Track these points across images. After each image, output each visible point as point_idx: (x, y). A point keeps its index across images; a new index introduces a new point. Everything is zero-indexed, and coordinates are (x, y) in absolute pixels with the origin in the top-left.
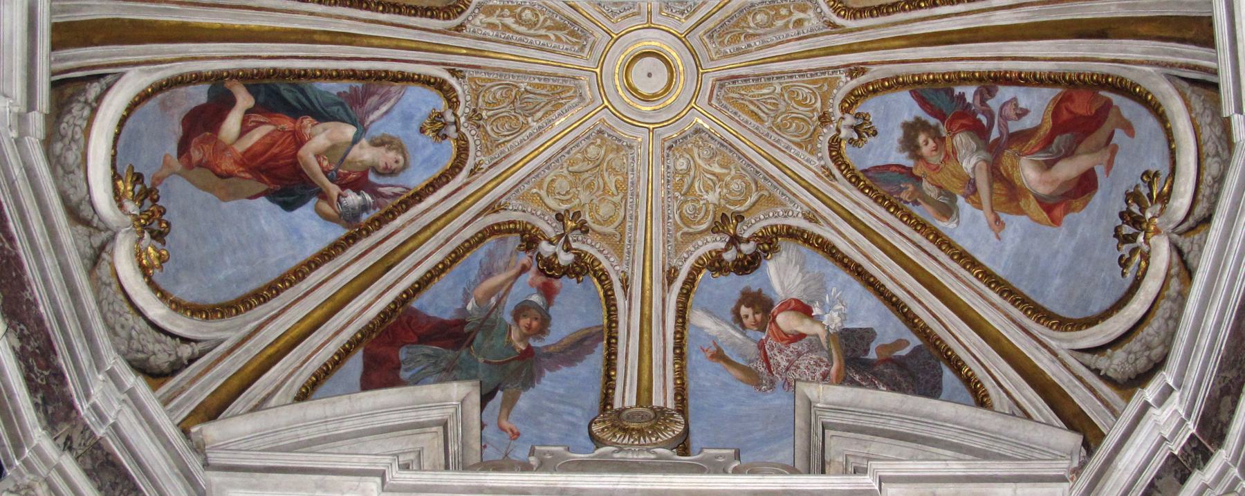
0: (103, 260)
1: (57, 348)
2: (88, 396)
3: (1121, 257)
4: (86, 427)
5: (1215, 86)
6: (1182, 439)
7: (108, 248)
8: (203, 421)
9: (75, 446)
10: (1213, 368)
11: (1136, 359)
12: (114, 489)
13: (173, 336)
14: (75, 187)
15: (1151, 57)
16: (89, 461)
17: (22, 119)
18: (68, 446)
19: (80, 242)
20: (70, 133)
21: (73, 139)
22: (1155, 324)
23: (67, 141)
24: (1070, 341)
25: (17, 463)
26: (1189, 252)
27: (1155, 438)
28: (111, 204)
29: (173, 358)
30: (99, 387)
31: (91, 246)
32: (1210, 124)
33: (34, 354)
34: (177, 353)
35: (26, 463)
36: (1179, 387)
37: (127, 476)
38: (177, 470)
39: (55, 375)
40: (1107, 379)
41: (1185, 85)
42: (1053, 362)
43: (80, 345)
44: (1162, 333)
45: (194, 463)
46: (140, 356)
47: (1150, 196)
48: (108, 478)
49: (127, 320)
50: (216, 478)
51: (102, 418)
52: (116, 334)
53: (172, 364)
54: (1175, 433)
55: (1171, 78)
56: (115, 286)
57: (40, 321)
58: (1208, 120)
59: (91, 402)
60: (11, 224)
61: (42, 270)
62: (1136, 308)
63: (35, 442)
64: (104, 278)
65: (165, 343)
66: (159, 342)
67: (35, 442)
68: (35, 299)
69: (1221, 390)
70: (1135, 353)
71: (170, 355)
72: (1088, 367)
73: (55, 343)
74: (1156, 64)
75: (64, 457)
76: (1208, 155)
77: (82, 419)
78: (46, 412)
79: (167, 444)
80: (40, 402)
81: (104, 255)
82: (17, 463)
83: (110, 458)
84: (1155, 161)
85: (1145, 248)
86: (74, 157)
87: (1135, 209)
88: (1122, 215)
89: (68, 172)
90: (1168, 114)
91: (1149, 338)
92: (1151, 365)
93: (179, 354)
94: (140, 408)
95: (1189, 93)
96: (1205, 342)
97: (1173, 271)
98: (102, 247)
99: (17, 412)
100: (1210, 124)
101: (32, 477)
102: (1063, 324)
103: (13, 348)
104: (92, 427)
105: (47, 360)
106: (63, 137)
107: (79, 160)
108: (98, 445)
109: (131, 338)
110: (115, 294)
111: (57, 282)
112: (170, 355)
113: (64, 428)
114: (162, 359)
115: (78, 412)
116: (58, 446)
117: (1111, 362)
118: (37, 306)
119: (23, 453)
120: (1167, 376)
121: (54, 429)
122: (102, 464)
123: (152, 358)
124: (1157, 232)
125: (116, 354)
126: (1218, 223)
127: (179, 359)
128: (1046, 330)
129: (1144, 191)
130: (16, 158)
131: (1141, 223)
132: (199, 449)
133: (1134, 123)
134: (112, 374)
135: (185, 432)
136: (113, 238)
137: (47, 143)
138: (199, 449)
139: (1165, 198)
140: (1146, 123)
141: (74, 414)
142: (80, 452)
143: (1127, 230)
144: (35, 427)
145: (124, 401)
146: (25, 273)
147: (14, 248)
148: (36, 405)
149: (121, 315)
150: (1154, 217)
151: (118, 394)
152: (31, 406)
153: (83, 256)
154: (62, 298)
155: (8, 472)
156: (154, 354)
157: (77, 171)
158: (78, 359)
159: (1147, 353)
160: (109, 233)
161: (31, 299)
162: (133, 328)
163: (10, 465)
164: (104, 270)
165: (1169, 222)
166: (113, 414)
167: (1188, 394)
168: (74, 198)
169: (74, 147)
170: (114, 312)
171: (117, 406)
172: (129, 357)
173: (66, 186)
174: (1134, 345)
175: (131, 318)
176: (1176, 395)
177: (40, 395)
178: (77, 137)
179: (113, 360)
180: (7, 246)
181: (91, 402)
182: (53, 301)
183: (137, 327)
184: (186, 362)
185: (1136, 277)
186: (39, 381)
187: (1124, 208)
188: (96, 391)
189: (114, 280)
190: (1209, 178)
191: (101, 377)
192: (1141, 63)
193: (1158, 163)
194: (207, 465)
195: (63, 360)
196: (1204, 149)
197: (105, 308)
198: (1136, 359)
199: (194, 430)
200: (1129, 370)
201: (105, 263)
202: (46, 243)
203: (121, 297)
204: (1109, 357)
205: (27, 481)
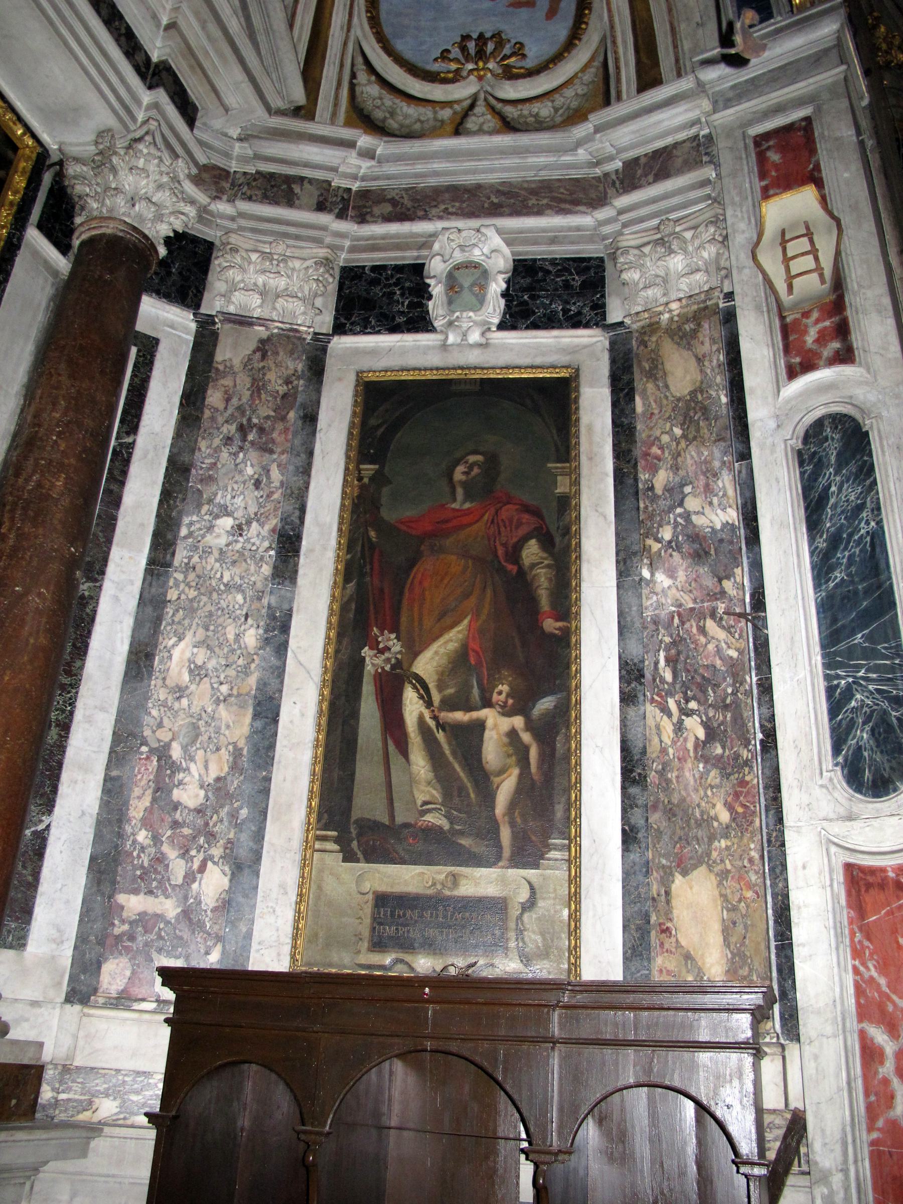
3: (447, 51)
5: (607, 103)
6: (345, 184)
10: (405, 183)
11: (378, 107)
15: (616, 19)
22: (410, 111)
24: (365, 36)
26: (474, 115)
27: (335, 162)
32: (577, 94)
36: (379, 162)
40: (352, 88)
41: (601, 58)
42: (342, 28)
44: (407, 122)
47: (505, 57)
54: (345, 176)
55: (603, 40)
58: (580, 92)
62: (416, 87)
69: (393, 199)
70: (383, 104)
72: (353, 65)
74: (612, 27)
76: (553, 101)
84: (534, 49)
85: (464, 74)
87: (490, 47)
88: (481, 36)
90: (574, 52)
91: (398, 111)
92: (380, 124)
95: (596, 64)
96: (420, 168)
97: (456, 106)
100: (577, 94)
102: (374, 21)
117: (366, 85)
120: (382, 147)
124: (480, 78)
126: (506, 140)
128: (363, 9)
129: (507, 50)
131: (481, 58)
133: (558, 16)
139: (509, 74)
140: (561, 29)
143: (471, 46)
150: (490, 70)
159: (388, 115)
165: (492, 87)
167: (377, 171)
174: (389, 100)
176: (373, 163)
185: (438, 73)
187: (488, 35)
190: (536, 110)
192: (609, 10)
193: (535, 53)
196: (557, 96)
198: (378, 107)
200: (369, 105)
204: (369, 81)
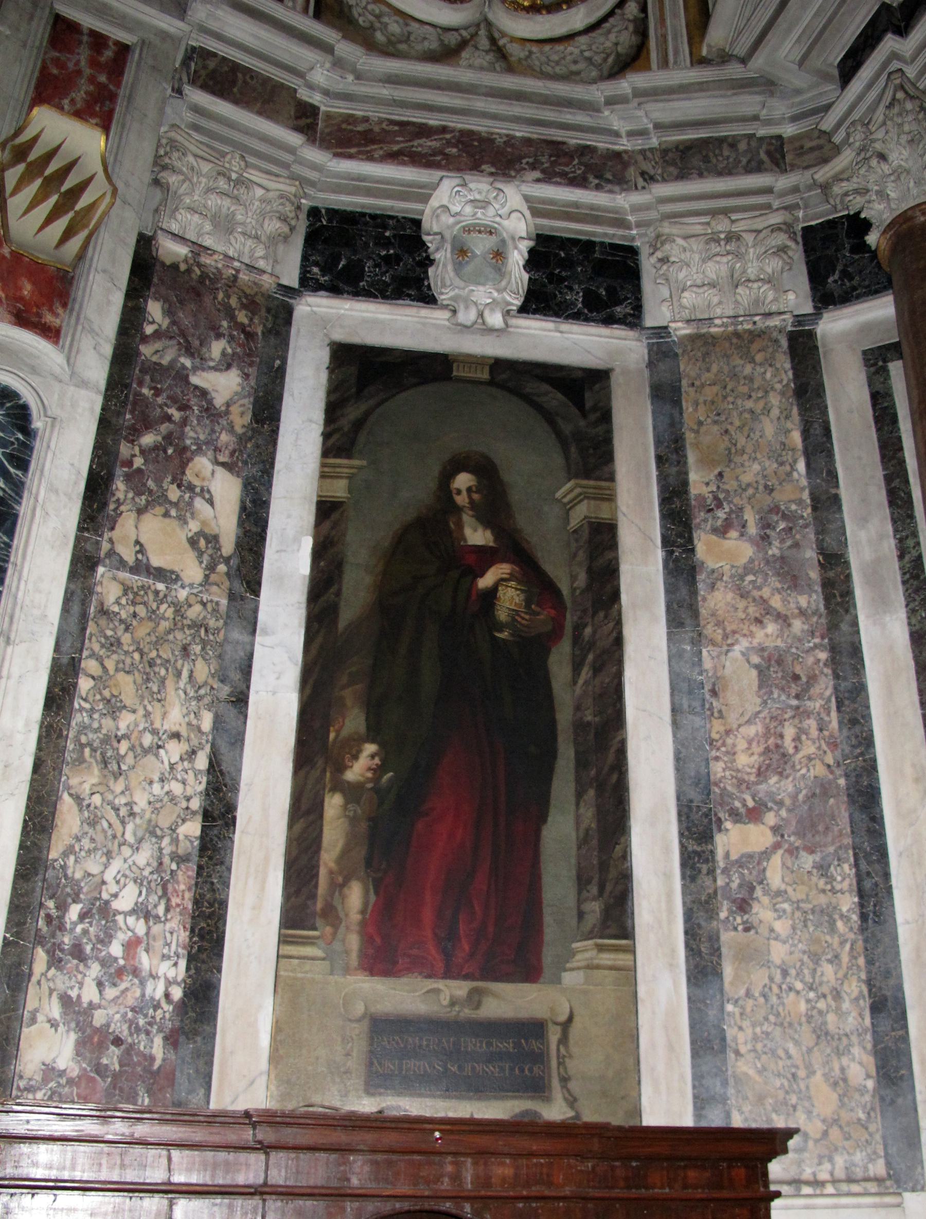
0: (504, 46)
1: (560, 139)
2: (617, 134)
4: (643, 152)
7: (496, 35)
8: (702, 41)
9: (652, 172)
12: (709, 162)
13: (611, 14)
14: (425, 38)
16: (671, 169)
17: (339, 64)
18: (650, 179)
19: (477, 62)
20: (371, 18)
21: (378, 17)
23: (377, 25)
25: (634, 232)
28: (455, 10)
29: (631, 27)
30: (614, 120)
31: (487, 52)
33: (553, 164)
34: (629, 21)
35: (639, 225)
37: (705, 142)
38: (729, 93)
39: (582, 155)
43: (569, 116)
45: (734, 70)
46: (610, 60)
48: (696, 161)
49: (571, 54)
50: (758, 62)
51: (643, 133)
52: (578, 73)
53: (636, 32)
56: (535, 49)
57: (528, 141)
59: (624, 134)
60: (431, 122)
61: (484, 115)
63: (627, 206)
64: (522, 55)
65: (614, 26)
66: (609, 32)
67: (627, 206)
68: (507, 136)
71: (626, 28)
73: (555, 138)
75: (653, 191)
77: (633, 151)
78: (608, 181)
79: (701, 87)
80: (597, 181)
81: (501, 42)
82: (634, 232)
83: (681, 147)
86: (395, 25)
89: (406, 38)
93: (631, 18)
94: (654, 94)
98: (493, 41)
99: (592, 207)
101: (652, 229)
103: (538, 180)
104: (647, 147)
105: (566, 154)
106: (372, 27)
107: (401, 21)
108: (665, 152)
109: (589, 60)
110: (542, 52)
111: (502, 107)
112: (626, 28)
113: (632, 172)
114: (625, 39)
115: (626, 152)
116: (644, 188)
118: (513, 137)
119: (630, 222)
121: (627, 182)
122: (682, 158)
123: (620, 49)
125: (594, 87)
127: (635, 21)
130: (372, 86)
132: (724, 58)
134: (611, 102)
135: (699, 61)
136: (489, 24)
137: (370, 46)
138: (724, 58)
141: (625, 157)
142: (660, 171)
144: (615, 199)
145: (639, 104)
146: (479, 133)
147: (453, 131)
148: (598, 187)
149: (564, 58)
151: (630, 106)
152: (594, 193)
153: (491, 68)
154: (517, 109)
155: (637, 243)
156: (616, 44)
157: (409, 29)
158: (580, 126)
160: (482, 26)
161: (505, 139)
162: (582, 52)
163: (633, 239)
164: (515, 51)
166: (645, 121)
168: (434, 45)
169: (386, 19)
170: (557, 63)
171: (641, 113)
172: (605, 73)
173: (419, 47)
175: (572, 49)
177: (591, 178)
178: (377, 11)
179: (598, 92)
180: (448, 136)
181: (624, 134)
182: (517, 120)
183: (584, 47)
184: (643, 15)
186: (579, 172)
188: (616, 124)
189: (528, 45)
191: (607, 113)
194: (744, 61)
195: (574, 140)
197: (549, 69)
199: (704, 52)
201: (508, 46)
202: (462, 98)
203: (547, 48)
205: (653, 235)
